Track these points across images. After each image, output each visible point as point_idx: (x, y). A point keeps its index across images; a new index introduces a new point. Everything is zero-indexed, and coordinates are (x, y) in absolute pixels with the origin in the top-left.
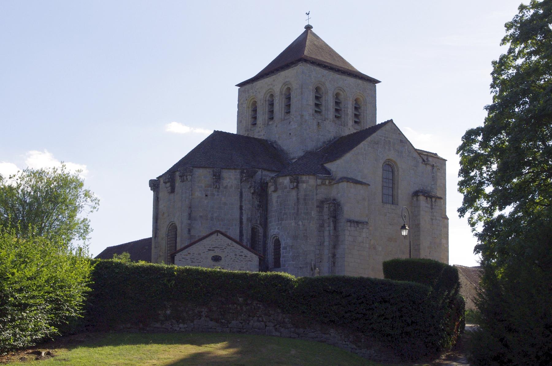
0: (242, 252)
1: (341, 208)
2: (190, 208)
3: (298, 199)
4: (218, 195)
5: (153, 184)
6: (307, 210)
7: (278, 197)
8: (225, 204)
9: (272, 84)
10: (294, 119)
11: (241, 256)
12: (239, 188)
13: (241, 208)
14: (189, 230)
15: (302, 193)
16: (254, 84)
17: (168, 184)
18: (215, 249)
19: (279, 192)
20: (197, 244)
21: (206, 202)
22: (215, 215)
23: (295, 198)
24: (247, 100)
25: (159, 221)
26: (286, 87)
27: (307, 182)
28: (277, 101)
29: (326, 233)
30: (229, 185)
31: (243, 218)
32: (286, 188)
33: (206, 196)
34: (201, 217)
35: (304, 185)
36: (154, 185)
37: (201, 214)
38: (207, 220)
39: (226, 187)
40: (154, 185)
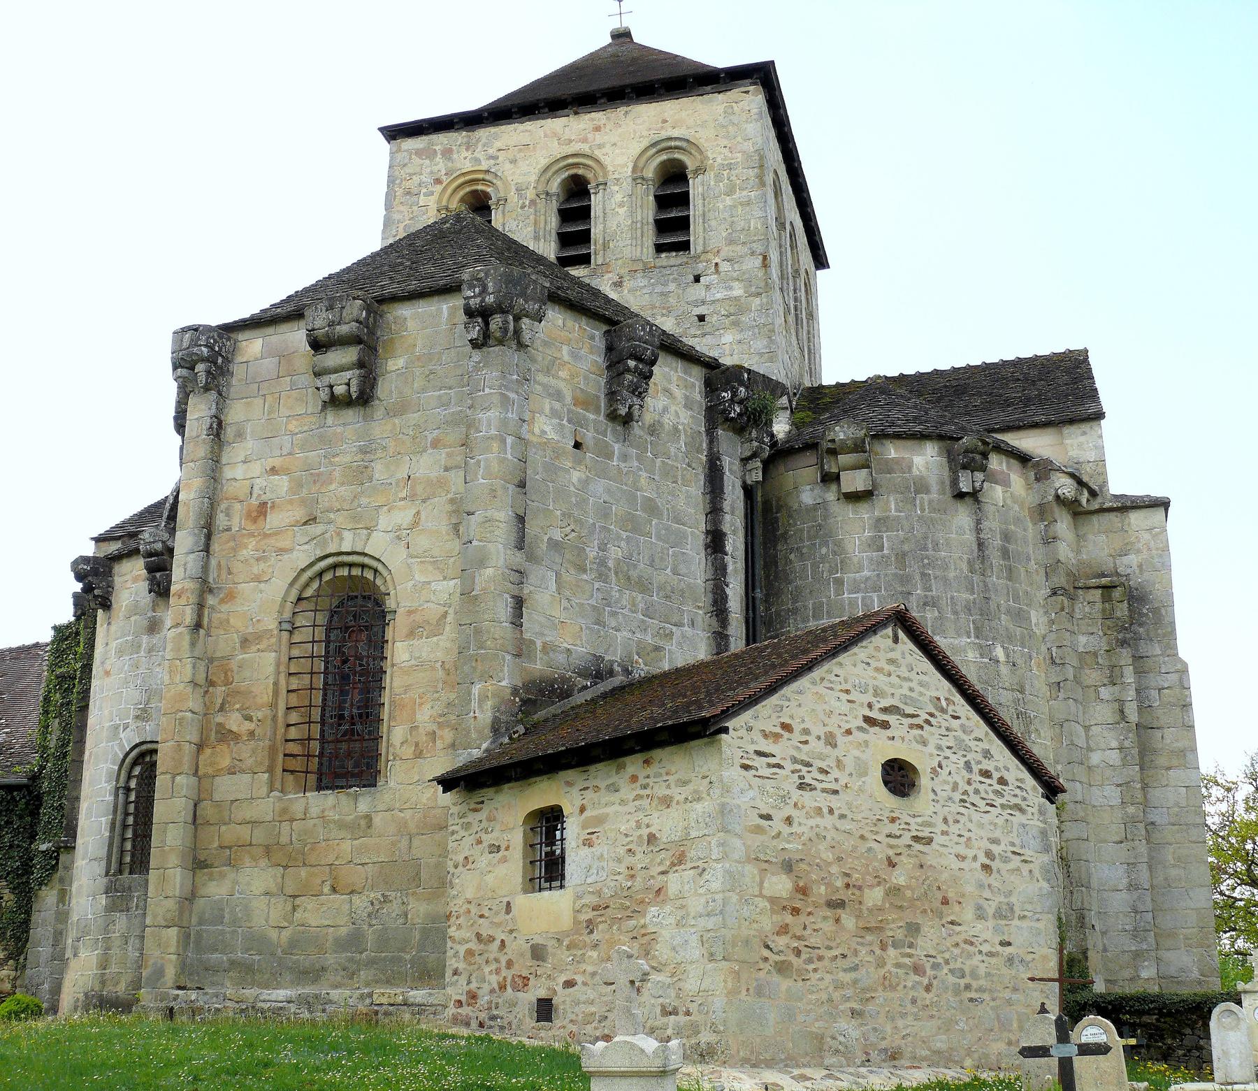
0: (987, 754)
1: (1156, 611)
2: (522, 485)
3: (981, 545)
4: (624, 457)
5: (211, 348)
6: (1016, 598)
7: (881, 523)
8: (652, 508)
9: (585, 140)
10: (724, 267)
11: (986, 774)
12: (699, 451)
13: (715, 542)
14: (519, 603)
15: (992, 524)
16: (483, 133)
17: (334, 358)
18: (892, 719)
19: (889, 504)
20: (816, 674)
21: (576, 476)
22: (615, 553)
23: (970, 537)
24: (438, 181)
25: (215, 547)
26: (664, 157)
27: (1006, 483)
28: (618, 197)
29: (1103, 713)
30: (668, 421)
31: (728, 591)
32: (921, 487)
33: (577, 445)
34: (554, 545)
35: (999, 489)
36: (206, 361)
37: (557, 535)
38: (585, 571)
39: (653, 430)
40: (206, 361)
